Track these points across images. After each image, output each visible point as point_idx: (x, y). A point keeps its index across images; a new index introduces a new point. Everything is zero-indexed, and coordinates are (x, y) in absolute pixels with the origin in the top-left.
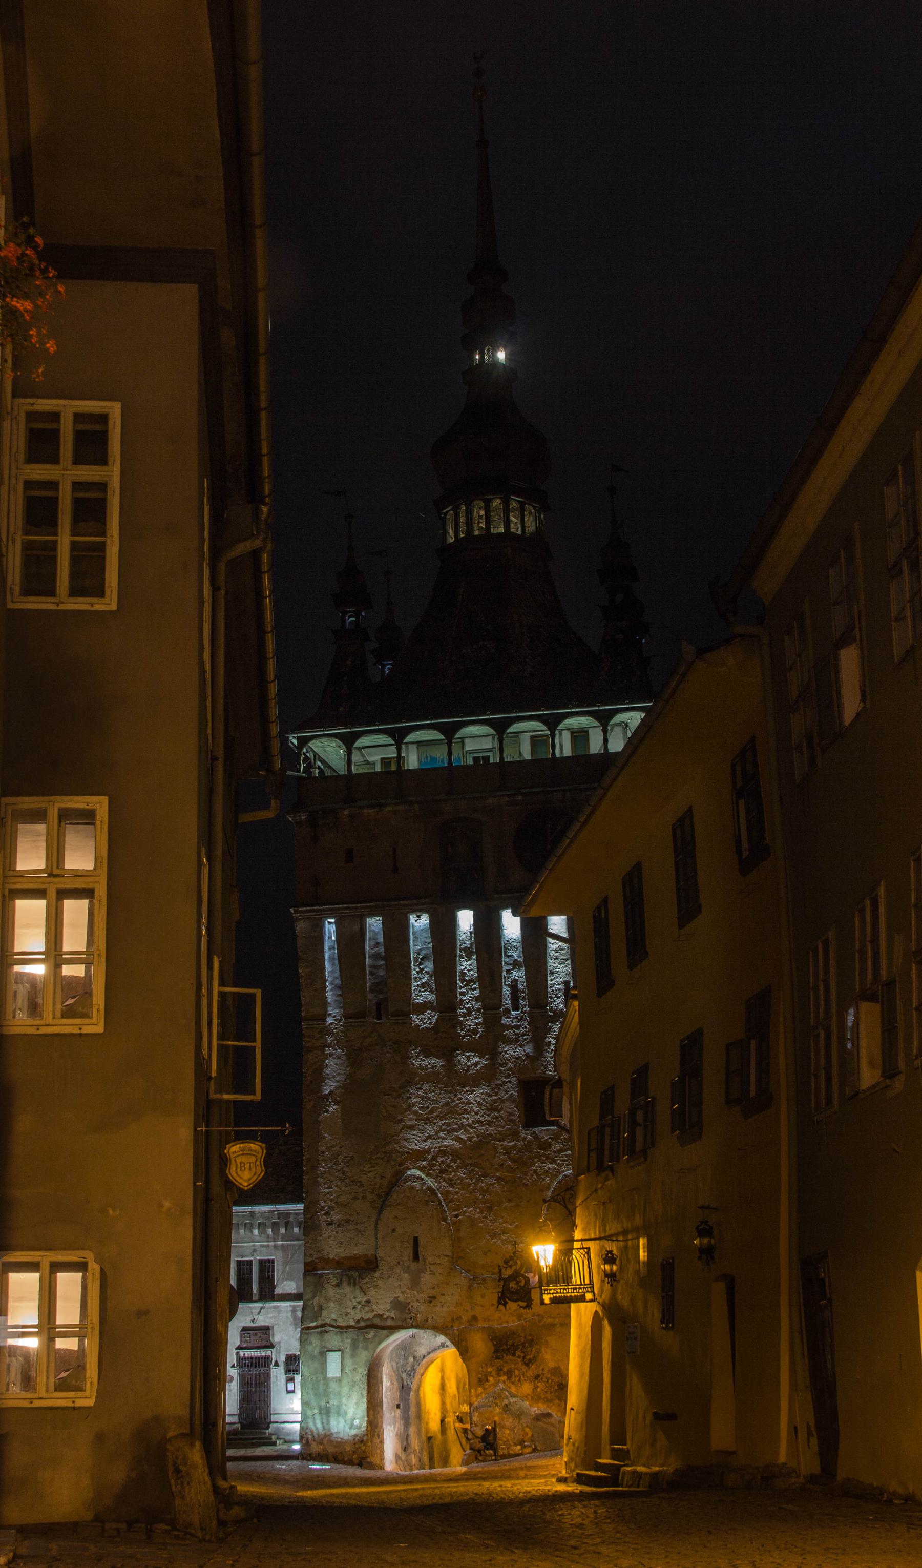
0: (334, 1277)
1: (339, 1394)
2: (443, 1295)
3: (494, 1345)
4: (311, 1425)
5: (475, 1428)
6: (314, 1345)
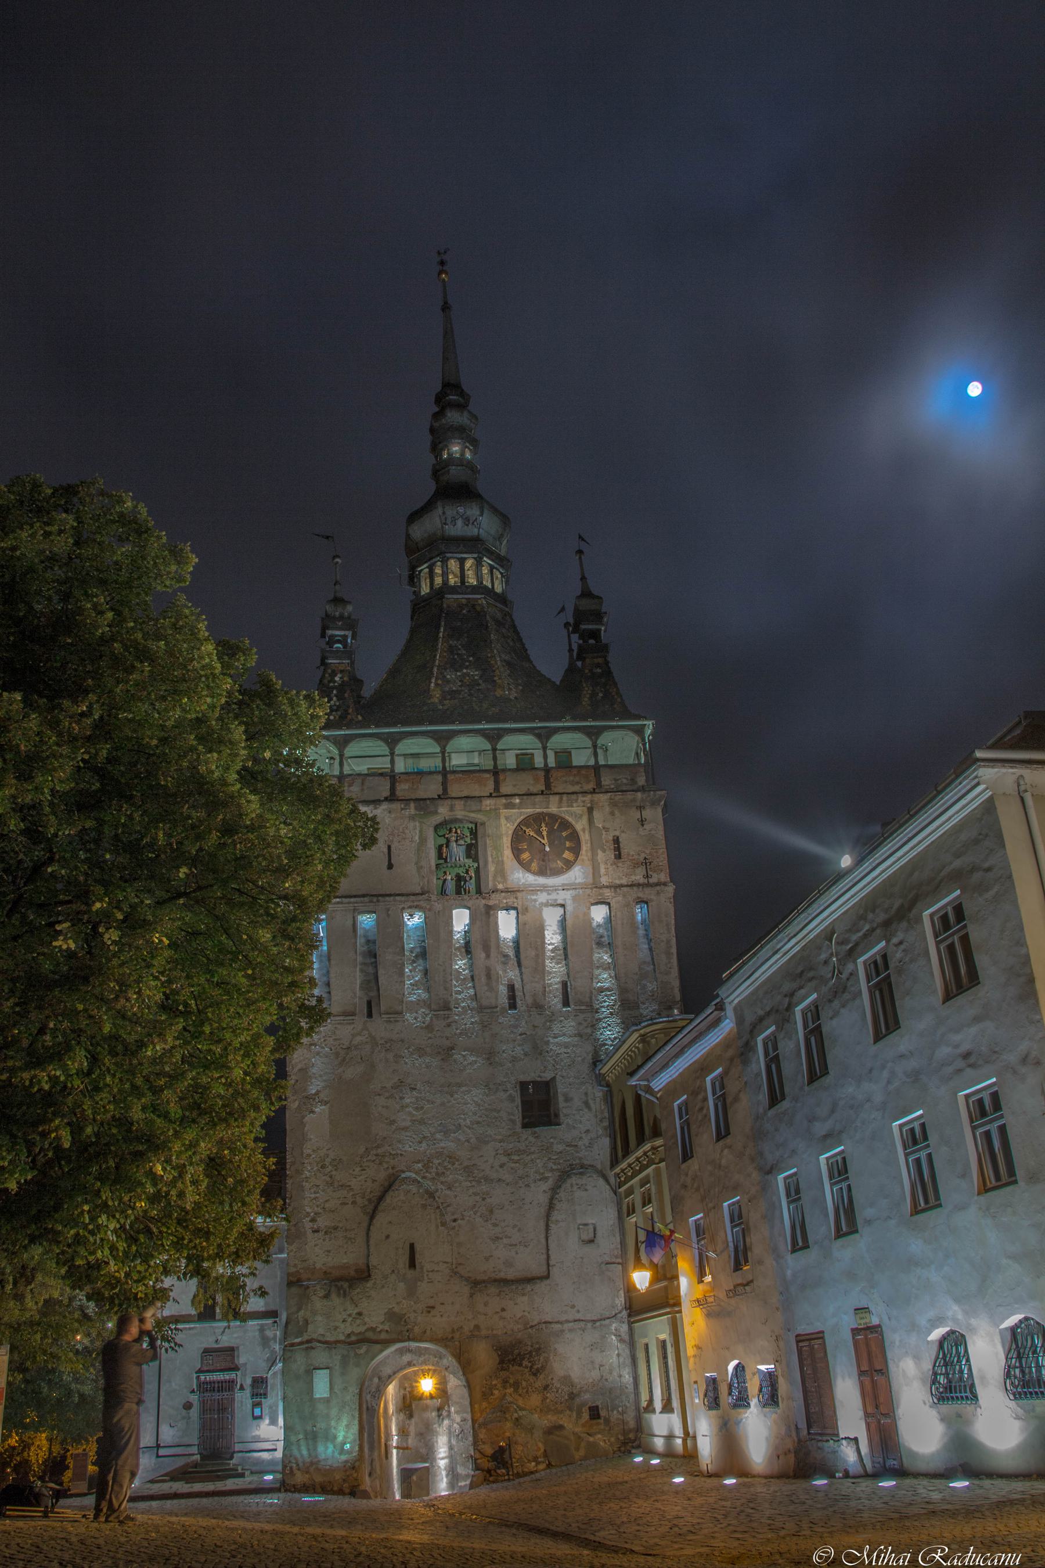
0: (321, 1288)
1: (327, 1417)
2: (443, 1304)
3: (499, 1356)
4: (296, 1452)
5: (483, 1447)
6: (299, 1363)
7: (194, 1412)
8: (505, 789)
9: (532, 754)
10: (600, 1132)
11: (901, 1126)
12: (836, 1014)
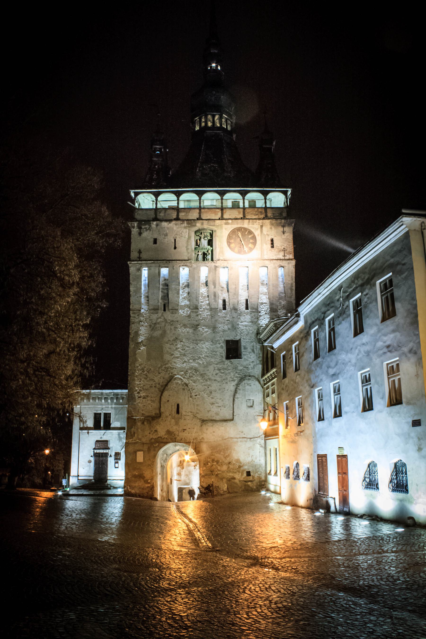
7: (92, 464)
8: (225, 216)
9: (239, 202)
10: (258, 362)
11: (361, 374)
12: (340, 323)
